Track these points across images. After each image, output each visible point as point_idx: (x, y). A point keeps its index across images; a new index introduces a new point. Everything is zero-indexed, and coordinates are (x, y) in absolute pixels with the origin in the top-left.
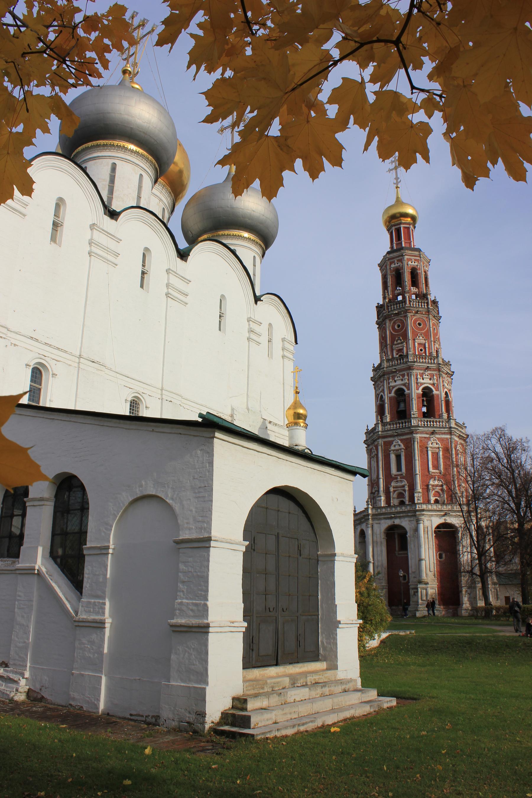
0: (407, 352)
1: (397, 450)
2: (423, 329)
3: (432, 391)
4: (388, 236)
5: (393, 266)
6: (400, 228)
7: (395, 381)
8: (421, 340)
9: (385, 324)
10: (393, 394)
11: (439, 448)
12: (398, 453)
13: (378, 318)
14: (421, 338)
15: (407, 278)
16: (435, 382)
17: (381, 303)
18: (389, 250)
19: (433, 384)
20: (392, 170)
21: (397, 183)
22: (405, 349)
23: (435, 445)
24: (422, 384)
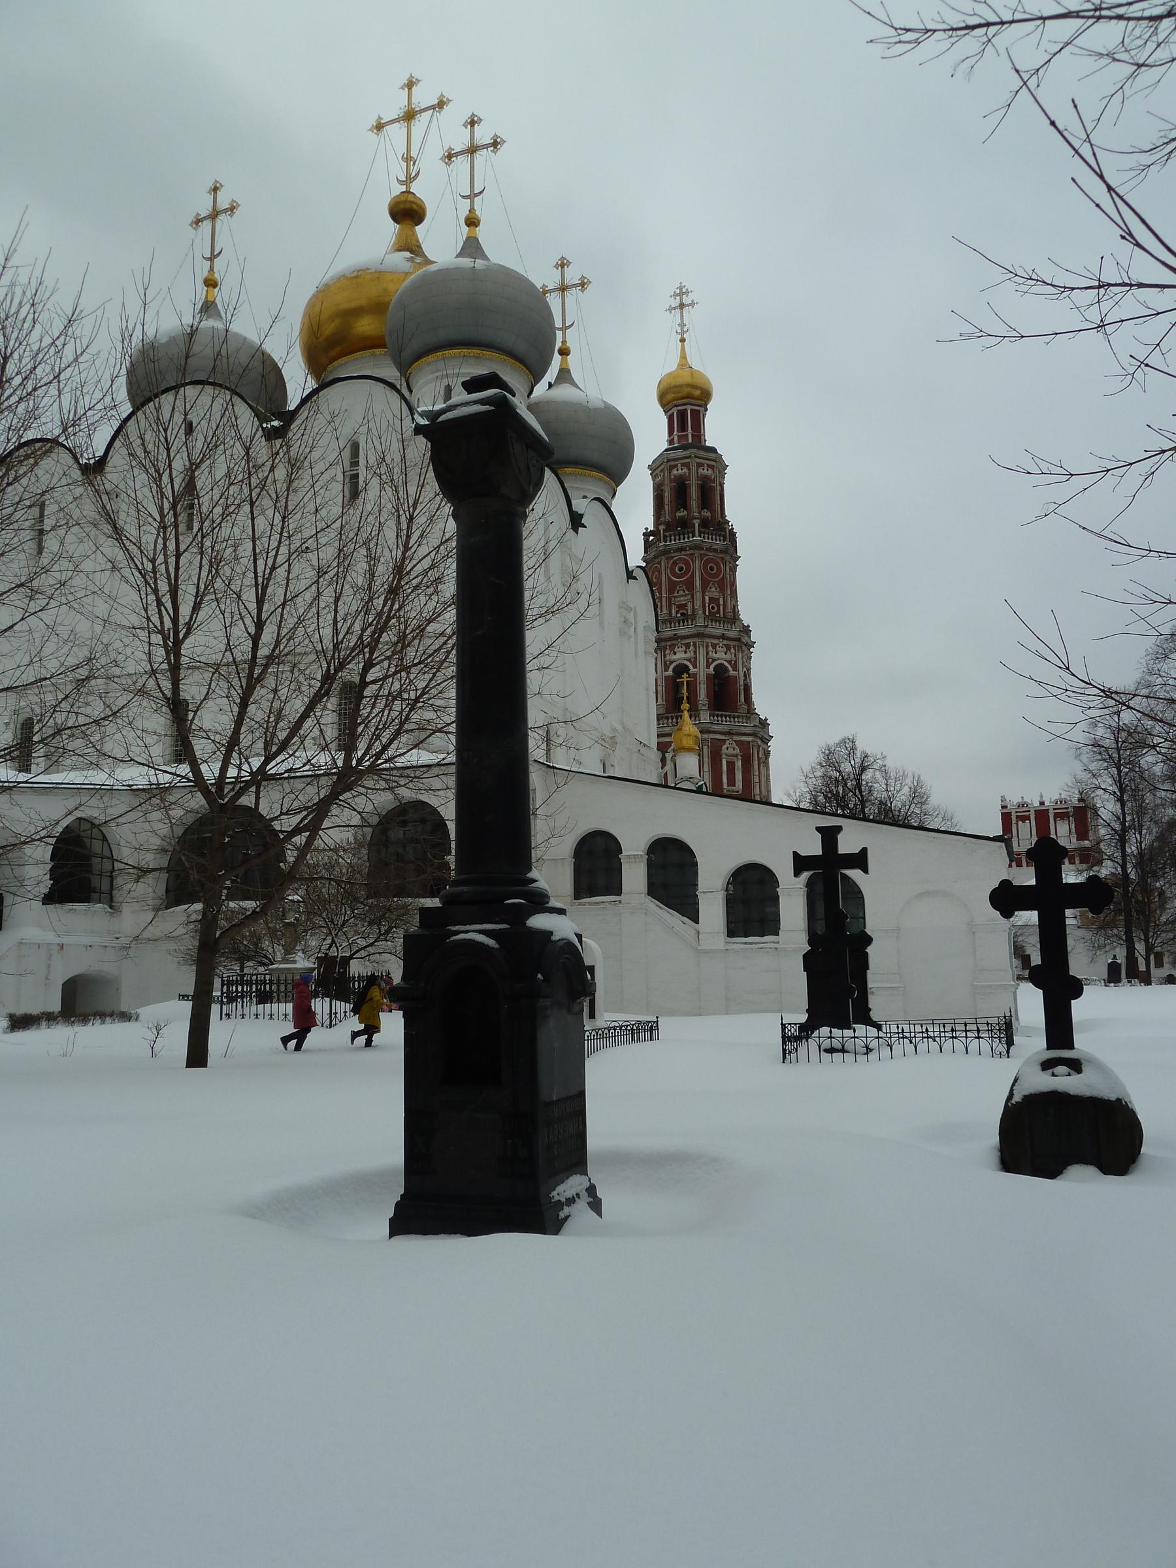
0: (693, 611)
2: (717, 575)
4: (666, 420)
5: (675, 472)
8: (714, 592)
9: (660, 563)
10: (670, 673)
13: (646, 552)
15: (694, 493)
17: (651, 528)
18: (666, 446)
20: (675, 309)
21: (683, 332)
22: (689, 605)
23: (731, 751)
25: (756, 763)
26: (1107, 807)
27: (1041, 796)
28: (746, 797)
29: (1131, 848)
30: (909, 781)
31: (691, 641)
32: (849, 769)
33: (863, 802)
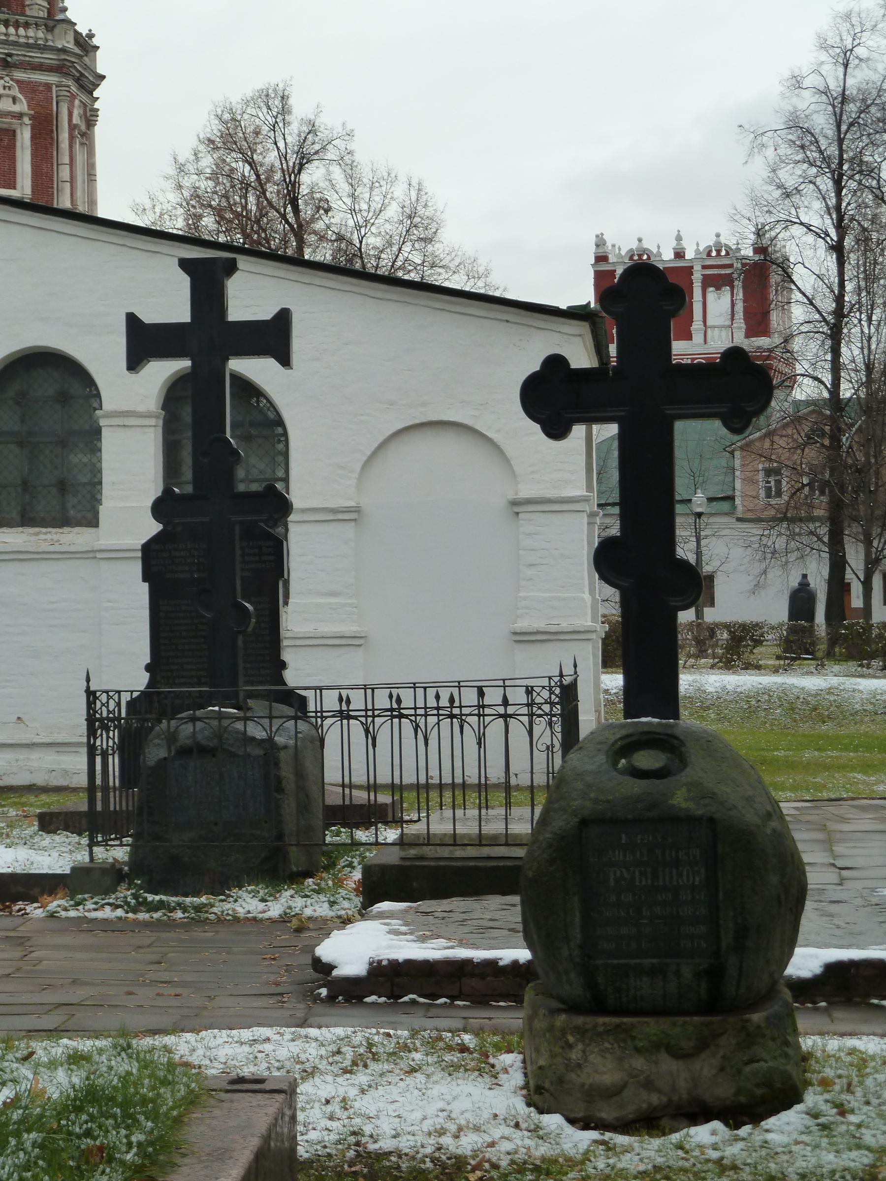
25: (64, 136)
26: (810, 262)
27: (679, 238)
28: (40, 206)
29: (851, 352)
30: (399, 191)
32: (272, 157)
33: (299, 231)
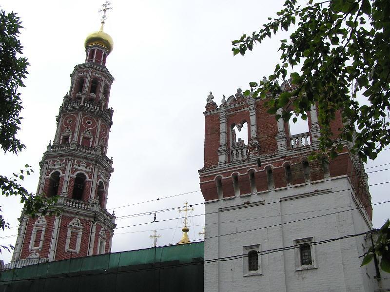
1: (39, 226)
3: (86, 177)
6: (95, 49)
7: (55, 166)
11: (79, 229)
12: (40, 229)
14: (87, 133)
15: (87, 85)
16: (90, 170)
19: (88, 173)
24: (77, 170)
31: (65, 158)
